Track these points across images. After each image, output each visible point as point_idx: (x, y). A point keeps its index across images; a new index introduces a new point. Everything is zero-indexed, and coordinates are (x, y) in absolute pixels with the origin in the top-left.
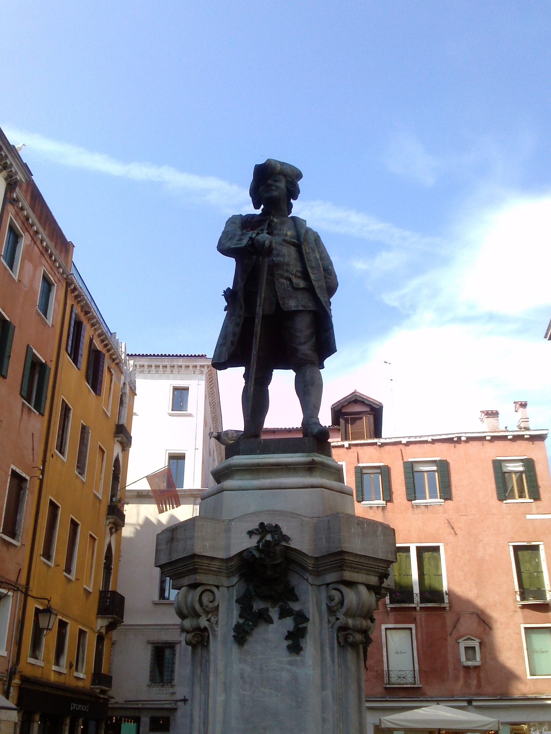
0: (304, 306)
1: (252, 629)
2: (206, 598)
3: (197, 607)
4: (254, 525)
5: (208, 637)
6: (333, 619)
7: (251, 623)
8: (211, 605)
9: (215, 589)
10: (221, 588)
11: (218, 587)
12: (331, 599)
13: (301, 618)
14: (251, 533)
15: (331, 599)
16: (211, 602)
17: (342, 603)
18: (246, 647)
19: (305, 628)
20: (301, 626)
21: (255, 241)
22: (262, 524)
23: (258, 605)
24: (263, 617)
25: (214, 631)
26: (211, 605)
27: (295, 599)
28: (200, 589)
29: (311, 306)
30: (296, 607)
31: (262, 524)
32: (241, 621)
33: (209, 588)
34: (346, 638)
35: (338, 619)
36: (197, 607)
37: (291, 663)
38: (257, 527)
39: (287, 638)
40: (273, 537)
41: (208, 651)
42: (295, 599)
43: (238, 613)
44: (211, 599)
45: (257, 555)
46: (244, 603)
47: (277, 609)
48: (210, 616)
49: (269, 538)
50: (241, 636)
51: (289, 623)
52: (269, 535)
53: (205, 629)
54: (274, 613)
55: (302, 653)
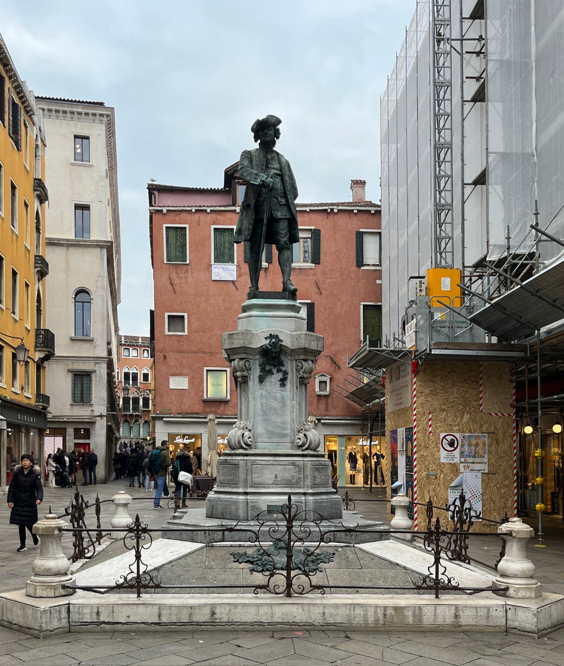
2: (247, 364)
3: (244, 367)
6: (298, 374)
12: (298, 366)
13: (285, 373)
15: (298, 366)
18: (263, 384)
22: (271, 334)
23: (268, 368)
24: (270, 372)
27: (283, 365)
30: (283, 369)
31: (271, 334)
32: (261, 374)
34: (303, 381)
37: (281, 390)
39: (280, 381)
41: (248, 385)
42: (283, 365)
47: (276, 369)
49: (274, 340)
50: (261, 380)
51: (280, 375)
53: (247, 377)
54: (275, 371)
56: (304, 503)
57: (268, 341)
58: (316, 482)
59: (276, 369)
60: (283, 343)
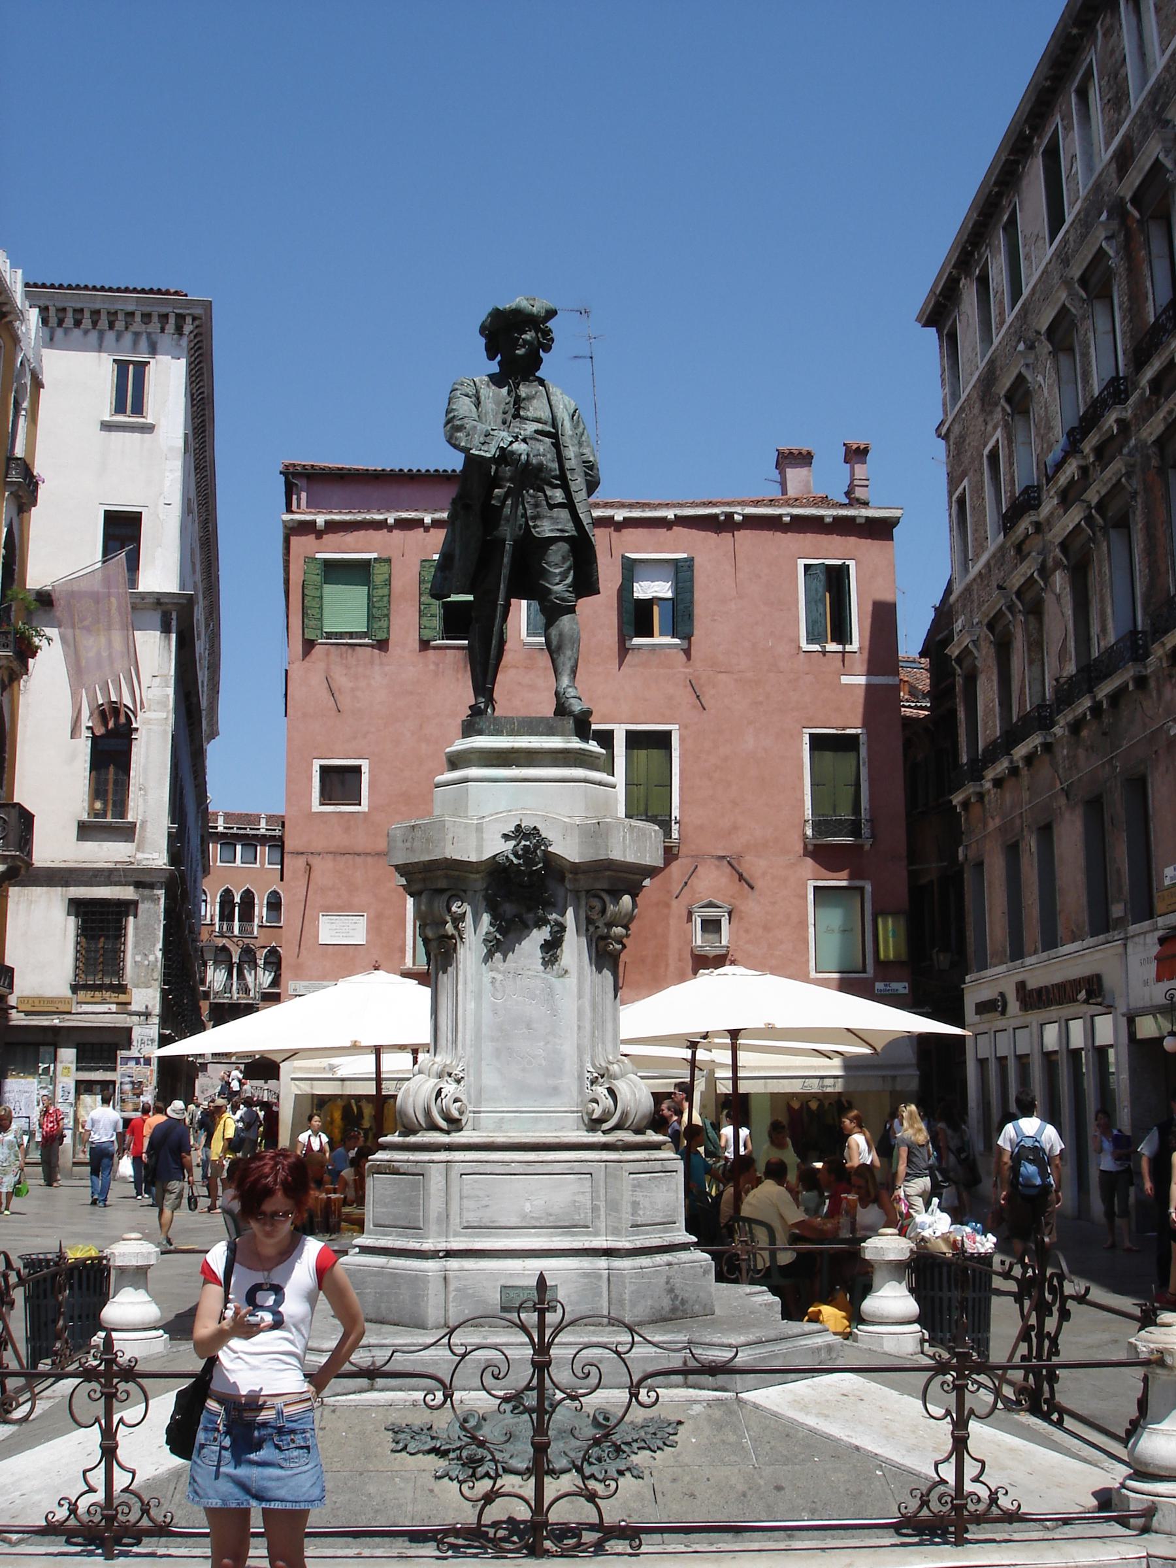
4: (510, 828)
12: (592, 908)
14: (506, 837)
29: (570, 527)
32: (492, 929)
35: (597, 927)
45: (515, 861)
52: (526, 837)
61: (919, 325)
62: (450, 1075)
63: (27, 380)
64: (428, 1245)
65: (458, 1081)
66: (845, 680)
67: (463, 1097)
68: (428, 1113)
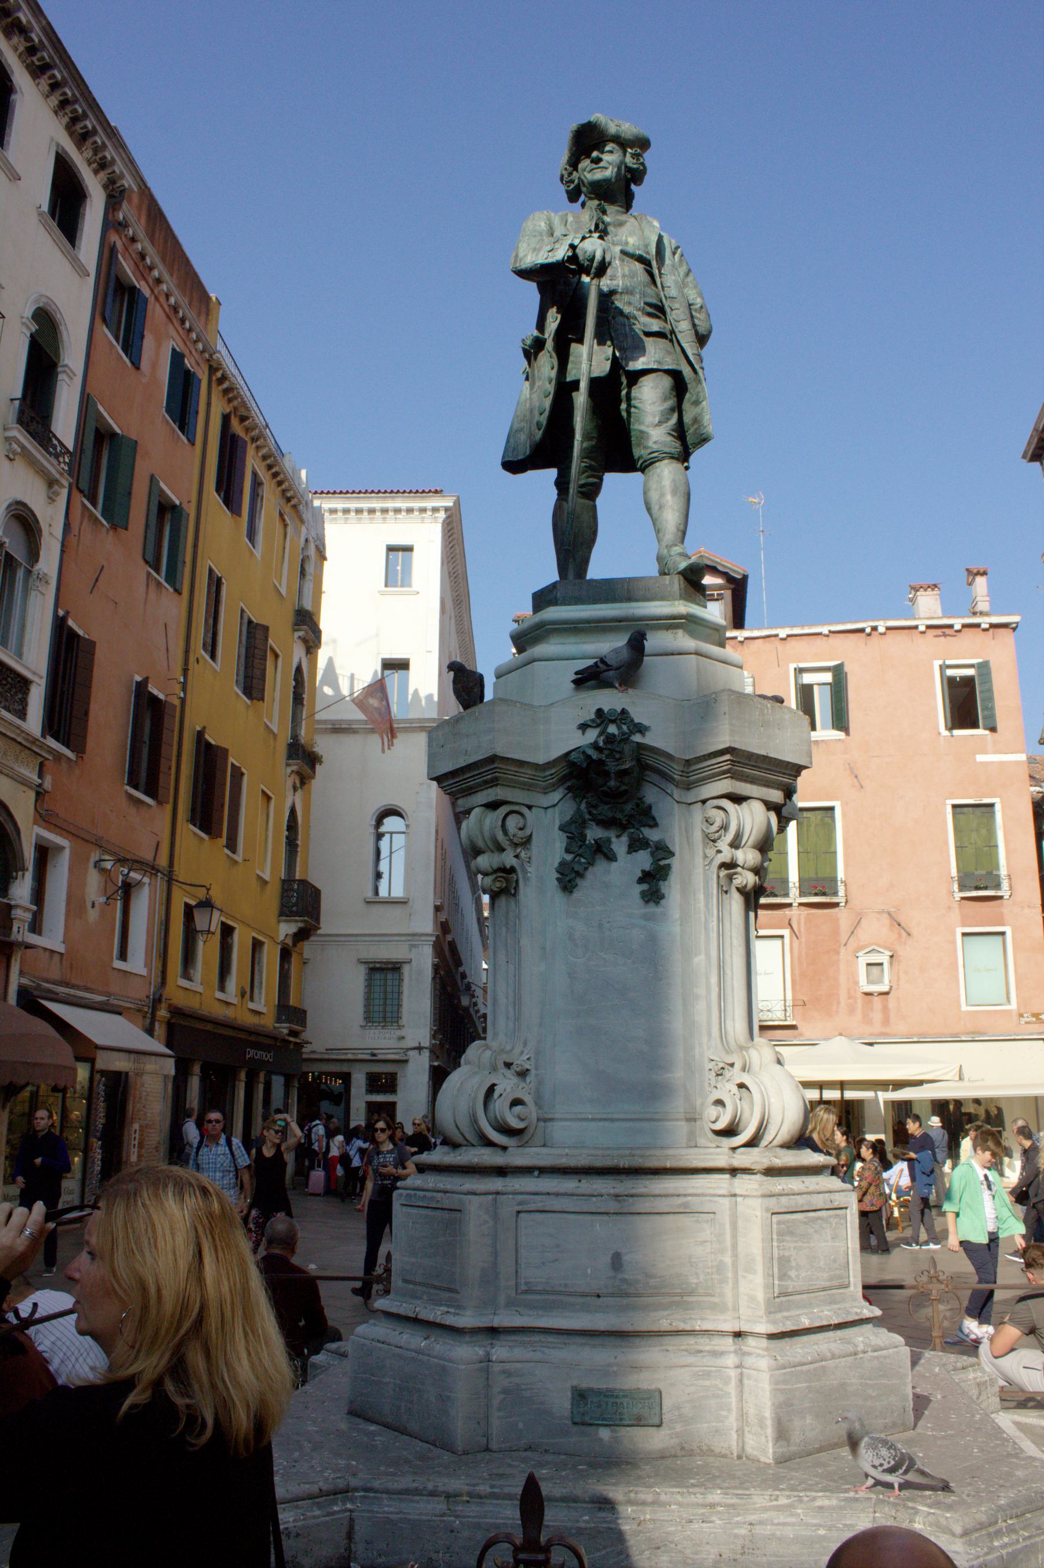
0: (659, 363)
1: (586, 869)
2: (512, 823)
3: (500, 836)
5: (517, 882)
7: (583, 860)
8: (520, 834)
9: (525, 810)
10: (534, 809)
11: (530, 807)
12: (709, 822)
13: (662, 851)
14: (584, 727)
16: (521, 829)
17: (725, 827)
18: (577, 894)
19: (668, 867)
20: (662, 863)
21: (577, 251)
22: (599, 712)
23: (594, 833)
24: (602, 851)
25: (525, 872)
26: (520, 834)
27: (654, 824)
28: (503, 810)
30: (653, 835)
31: (599, 712)
32: (569, 857)
33: (516, 808)
35: (719, 851)
36: (500, 836)
38: (593, 716)
40: (619, 728)
41: (517, 902)
42: (654, 824)
43: (564, 845)
44: (521, 825)
46: (573, 830)
47: (625, 839)
48: (518, 850)
50: (568, 879)
51: (643, 860)
53: (512, 870)
54: (620, 845)
55: (663, 902)
56: (733, 1383)
57: (592, 735)
58: (790, 1285)
59: (625, 839)
60: (648, 740)
61: (1025, 461)
62: (508, 1065)
63: (312, 551)
64: (466, 1320)
65: (523, 1074)
66: (980, 758)
67: (527, 1098)
68: (474, 1121)
